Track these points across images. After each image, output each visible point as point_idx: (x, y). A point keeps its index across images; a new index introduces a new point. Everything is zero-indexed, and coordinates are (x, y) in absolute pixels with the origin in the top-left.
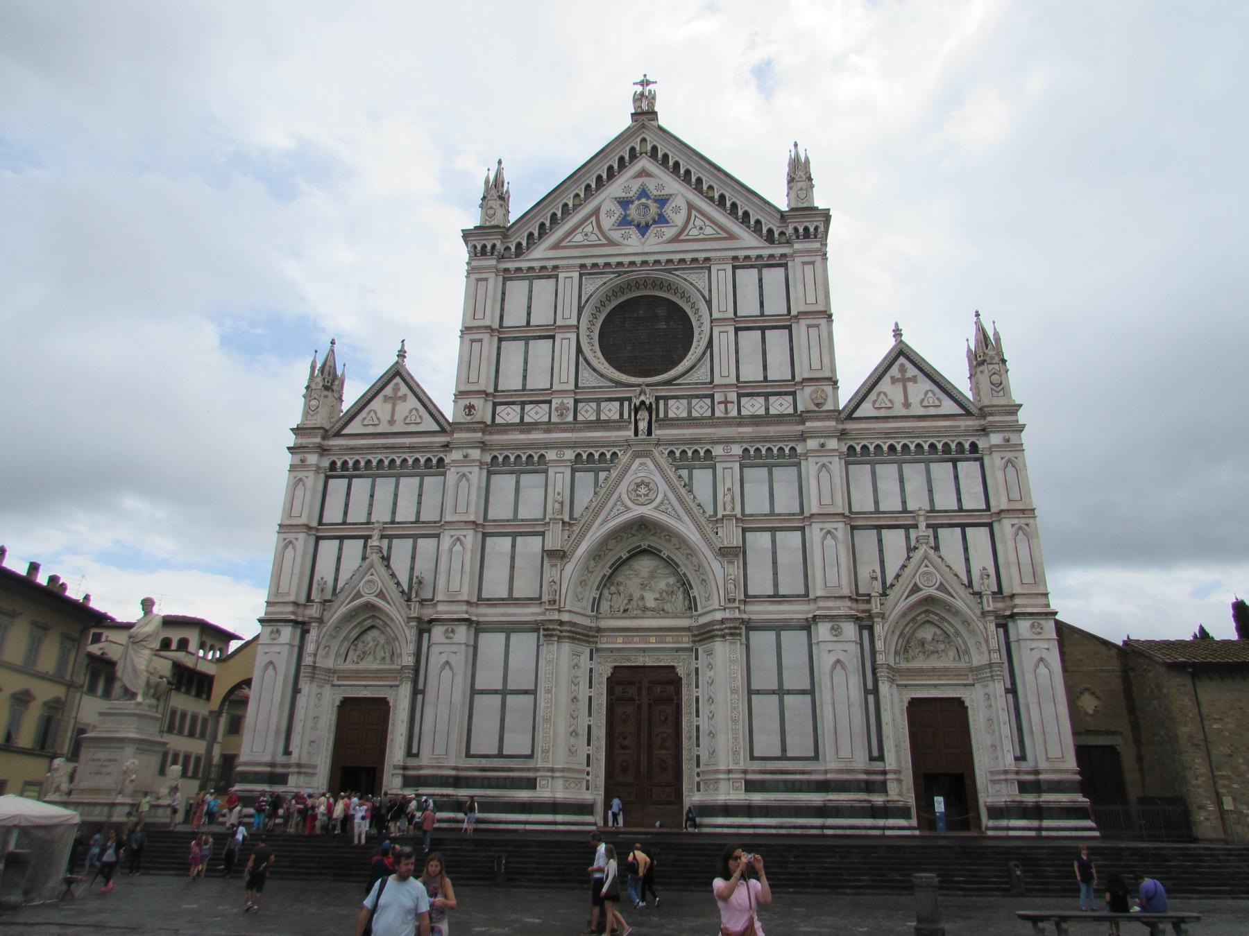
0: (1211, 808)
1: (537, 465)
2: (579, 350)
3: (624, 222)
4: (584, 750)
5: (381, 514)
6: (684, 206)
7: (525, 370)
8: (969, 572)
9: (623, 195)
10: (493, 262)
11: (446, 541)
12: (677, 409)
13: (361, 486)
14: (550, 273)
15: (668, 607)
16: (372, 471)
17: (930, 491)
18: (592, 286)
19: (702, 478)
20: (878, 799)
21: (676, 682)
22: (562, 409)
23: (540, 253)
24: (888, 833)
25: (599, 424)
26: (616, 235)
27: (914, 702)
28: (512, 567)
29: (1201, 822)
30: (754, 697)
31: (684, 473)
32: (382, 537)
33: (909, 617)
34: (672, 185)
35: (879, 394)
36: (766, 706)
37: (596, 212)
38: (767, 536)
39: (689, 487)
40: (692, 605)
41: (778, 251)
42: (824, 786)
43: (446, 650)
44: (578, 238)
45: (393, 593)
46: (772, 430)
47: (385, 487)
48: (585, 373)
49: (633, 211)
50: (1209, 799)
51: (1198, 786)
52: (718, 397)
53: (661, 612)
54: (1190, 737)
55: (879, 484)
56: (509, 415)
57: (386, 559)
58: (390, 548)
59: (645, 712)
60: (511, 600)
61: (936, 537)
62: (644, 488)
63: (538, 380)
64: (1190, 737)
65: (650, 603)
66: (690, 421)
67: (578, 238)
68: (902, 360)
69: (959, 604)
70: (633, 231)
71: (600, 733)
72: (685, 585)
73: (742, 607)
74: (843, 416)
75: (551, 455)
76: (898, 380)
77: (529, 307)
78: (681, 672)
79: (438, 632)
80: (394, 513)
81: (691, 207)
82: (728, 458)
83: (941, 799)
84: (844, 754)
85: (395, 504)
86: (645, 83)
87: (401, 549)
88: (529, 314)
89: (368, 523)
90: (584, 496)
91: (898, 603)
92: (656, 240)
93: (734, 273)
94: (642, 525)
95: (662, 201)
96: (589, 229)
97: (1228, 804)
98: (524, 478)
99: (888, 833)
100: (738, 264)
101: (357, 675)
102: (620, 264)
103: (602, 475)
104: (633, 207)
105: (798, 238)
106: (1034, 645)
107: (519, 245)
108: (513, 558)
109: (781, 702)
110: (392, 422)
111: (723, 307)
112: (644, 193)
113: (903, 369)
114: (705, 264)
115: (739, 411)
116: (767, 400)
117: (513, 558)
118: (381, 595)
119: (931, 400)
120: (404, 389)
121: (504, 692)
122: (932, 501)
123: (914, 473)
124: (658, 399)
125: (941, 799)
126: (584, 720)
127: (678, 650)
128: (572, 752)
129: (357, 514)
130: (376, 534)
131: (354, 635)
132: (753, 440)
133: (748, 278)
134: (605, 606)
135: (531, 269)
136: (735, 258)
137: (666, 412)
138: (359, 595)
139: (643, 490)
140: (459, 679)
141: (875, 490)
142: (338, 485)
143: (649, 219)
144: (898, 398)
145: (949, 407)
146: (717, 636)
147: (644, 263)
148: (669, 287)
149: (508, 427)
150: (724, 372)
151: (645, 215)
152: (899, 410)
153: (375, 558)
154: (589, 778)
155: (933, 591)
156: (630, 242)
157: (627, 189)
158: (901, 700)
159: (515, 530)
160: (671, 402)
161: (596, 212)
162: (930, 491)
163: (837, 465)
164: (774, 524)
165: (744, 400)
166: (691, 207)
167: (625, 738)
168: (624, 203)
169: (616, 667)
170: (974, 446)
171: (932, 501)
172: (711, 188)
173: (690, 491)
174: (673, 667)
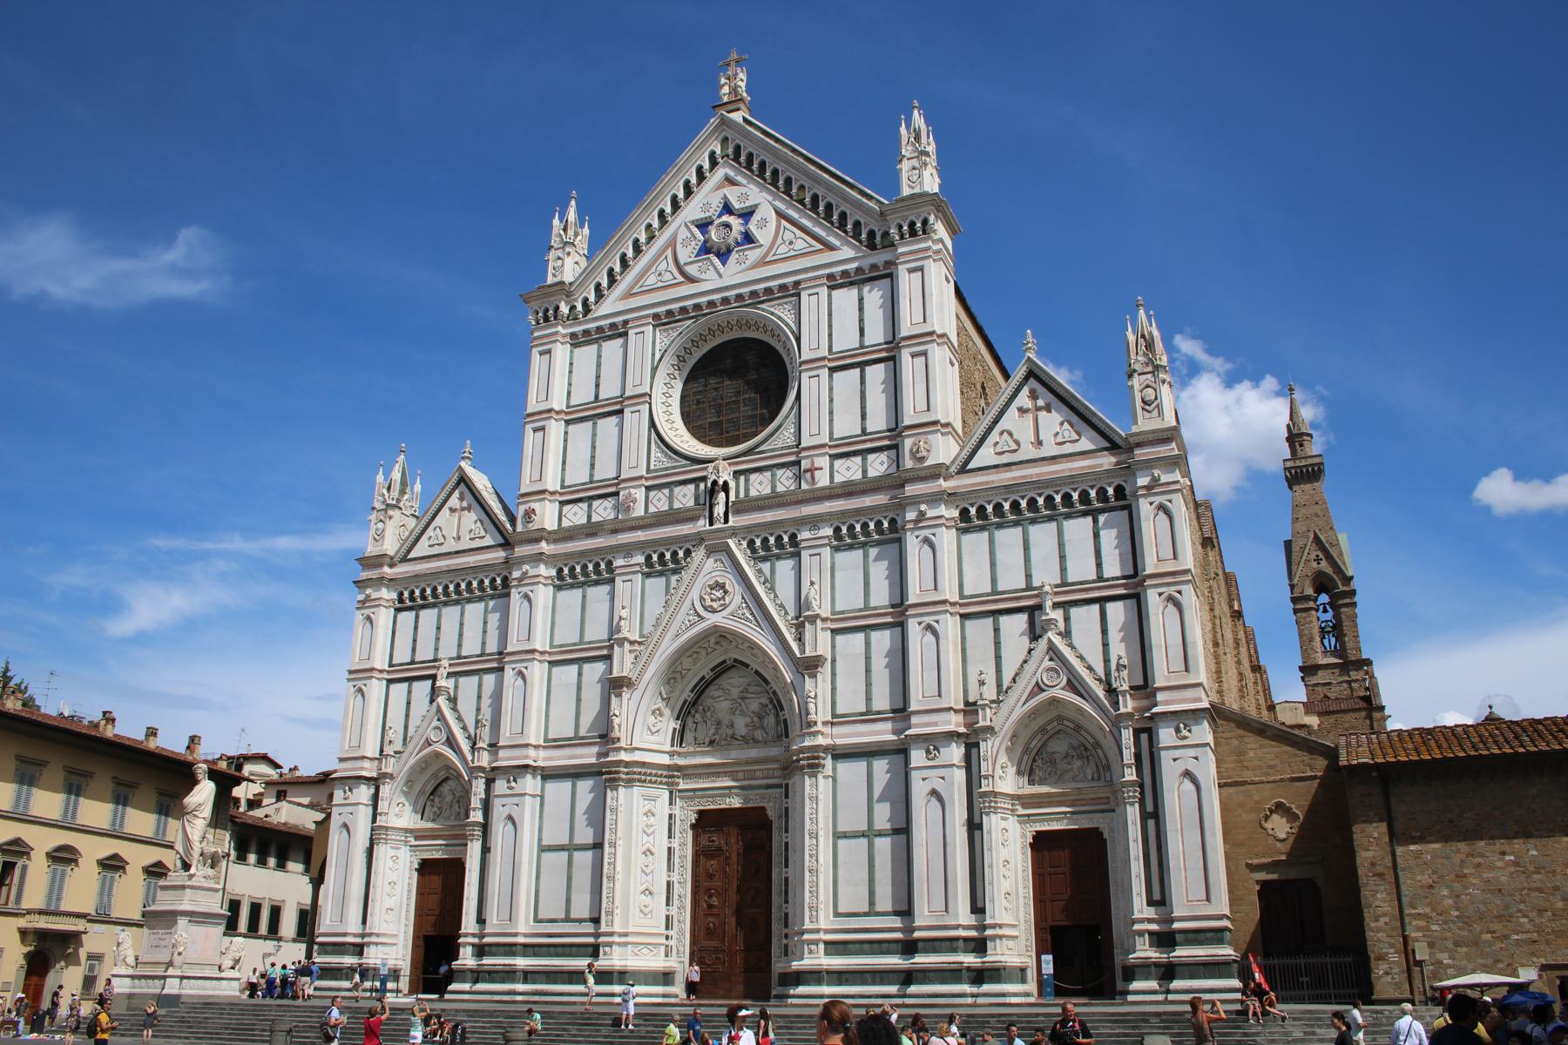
0: (1394, 957)
3: (706, 249)
4: (662, 911)
7: (593, 457)
8: (1107, 661)
9: (703, 215)
12: (759, 485)
14: (618, 331)
15: (759, 735)
17: (1062, 557)
19: (785, 567)
21: (766, 825)
24: (980, 1000)
26: (692, 270)
28: (579, 700)
29: (1379, 978)
30: (841, 842)
31: (766, 567)
32: (450, 675)
33: (1035, 726)
35: (1002, 433)
37: (672, 243)
41: (880, 258)
44: (651, 280)
49: (714, 235)
50: (1392, 946)
51: (1379, 930)
52: (805, 464)
53: (750, 741)
54: (1373, 864)
55: (999, 556)
57: (453, 701)
58: (456, 687)
61: (1067, 619)
64: (1373, 864)
67: (651, 280)
68: (1032, 380)
71: (684, 891)
72: (778, 705)
73: (827, 730)
74: (953, 469)
76: (1027, 411)
77: (598, 377)
78: (771, 813)
80: (460, 646)
83: (1050, 957)
85: (461, 635)
88: (597, 386)
89: (435, 660)
91: (1015, 708)
92: (739, 268)
93: (830, 296)
95: (747, 215)
96: (663, 266)
99: (980, 1000)
100: (836, 282)
102: (697, 307)
103: (674, 578)
105: (902, 237)
106: (1177, 753)
107: (585, 302)
108: (579, 689)
109: (871, 846)
112: (727, 209)
114: (791, 292)
115: (832, 477)
116: (864, 460)
117: (579, 689)
119: (1066, 434)
122: (1063, 570)
123: (1043, 535)
124: (737, 474)
125: (1050, 957)
127: (768, 787)
129: (425, 653)
131: (429, 789)
132: (844, 514)
133: (846, 298)
135: (600, 329)
136: (831, 277)
137: (747, 490)
138: (428, 743)
139: (719, 594)
141: (993, 565)
143: (731, 241)
146: (802, 768)
147: (725, 301)
148: (757, 324)
152: (1028, 452)
153: (442, 701)
154: (670, 942)
158: (1023, 836)
160: (753, 477)
161: (672, 243)
162: (1062, 557)
165: (837, 463)
167: (710, 897)
169: (701, 813)
171: (1063, 570)
172: (802, 187)
173: (772, 589)
174: (763, 809)
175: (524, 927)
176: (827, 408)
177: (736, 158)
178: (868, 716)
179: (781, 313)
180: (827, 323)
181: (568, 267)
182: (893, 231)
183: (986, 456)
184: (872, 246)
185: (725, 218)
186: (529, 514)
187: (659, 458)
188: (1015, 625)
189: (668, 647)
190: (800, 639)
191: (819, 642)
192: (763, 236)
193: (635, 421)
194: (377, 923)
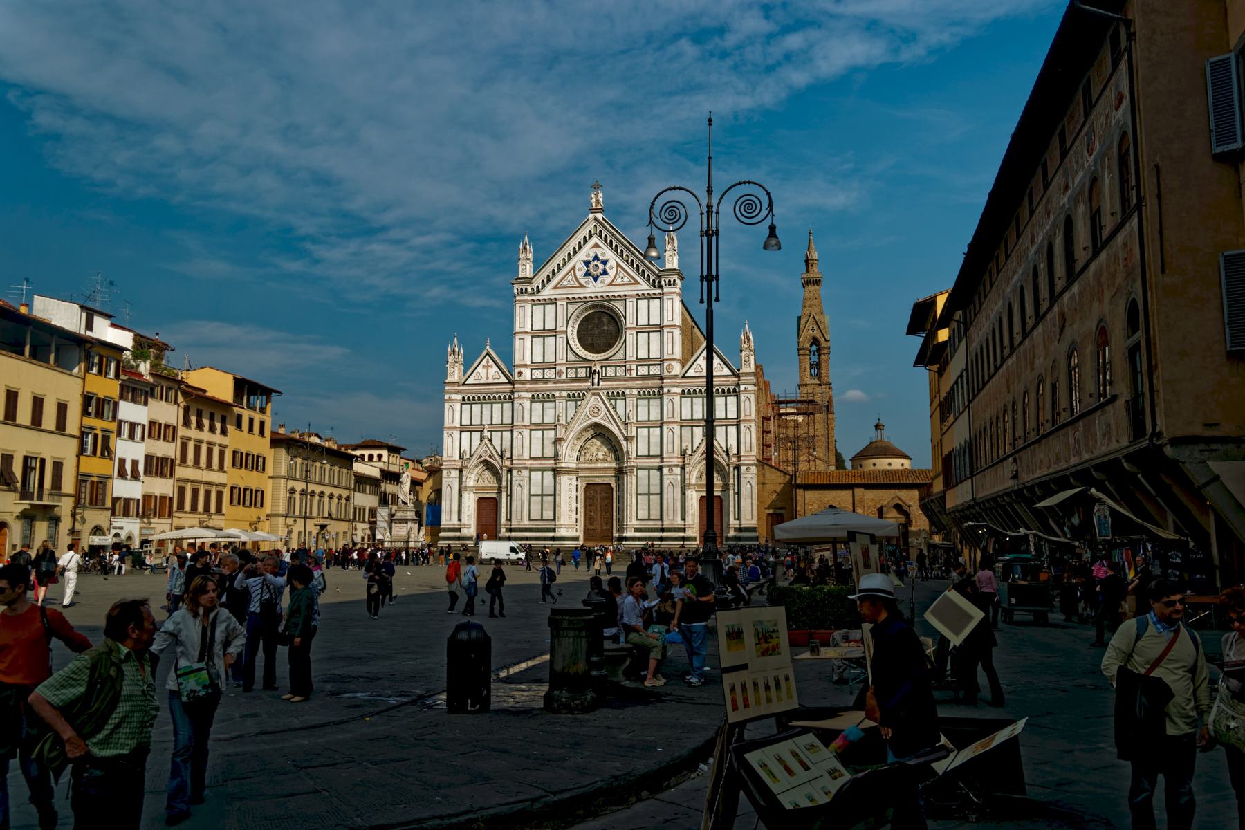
1: (554, 399)
2: (568, 343)
3: (587, 274)
4: (574, 517)
5: (486, 421)
6: (615, 265)
12: (610, 372)
13: (476, 407)
14: (553, 302)
16: (481, 401)
18: (571, 308)
19: (620, 403)
23: (548, 292)
25: (577, 380)
26: (583, 282)
36: (643, 500)
37: (573, 268)
39: (614, 408)
42: (662, 530)
43: (519, 479)
44: (565, 283)
46: (650, 383)
47: (486, 407)
53: (604, 460)
56: (538, 374)
59: (601, 501)
60: (543, 458)
62: (594, 409)
63: (550, 358)
65: (601, 456)
66: (616, 378)
67: (565, 283)
90: (571, 413)
94: (596, 425)
95: (605, 262)
98: (546, 405)
100: (639, 297)
101: (483, 488)
104: (591, 266)
111: (630, 322)
112: (596, 258)
114: (623, 299)
120: (491, 362)
121: (542, 495)
126: (574, 505)
128: (570, 517)
129: (476, 421)
142: (466, 407)
148: (608, 308)
149: (537, 381)
150: (631, 356)
156: (590, 285)
157: (587, 255)
159: (542, 427)
163: (677, 399)
164: (647, 424)
168: (587, 263)
175: (526, 523)
176: (635, 346)
178: (649, 456)
179: (619, 306)
180: (635, 313)
181: (526, 270)
183: (691, 373)
186: (520, 373)
187: (571, 357)
189: (577, 428)
190: (627, 430)
191: (632, 431)
192: (612, 273)
193: (561, 340)
194: (465, 520)
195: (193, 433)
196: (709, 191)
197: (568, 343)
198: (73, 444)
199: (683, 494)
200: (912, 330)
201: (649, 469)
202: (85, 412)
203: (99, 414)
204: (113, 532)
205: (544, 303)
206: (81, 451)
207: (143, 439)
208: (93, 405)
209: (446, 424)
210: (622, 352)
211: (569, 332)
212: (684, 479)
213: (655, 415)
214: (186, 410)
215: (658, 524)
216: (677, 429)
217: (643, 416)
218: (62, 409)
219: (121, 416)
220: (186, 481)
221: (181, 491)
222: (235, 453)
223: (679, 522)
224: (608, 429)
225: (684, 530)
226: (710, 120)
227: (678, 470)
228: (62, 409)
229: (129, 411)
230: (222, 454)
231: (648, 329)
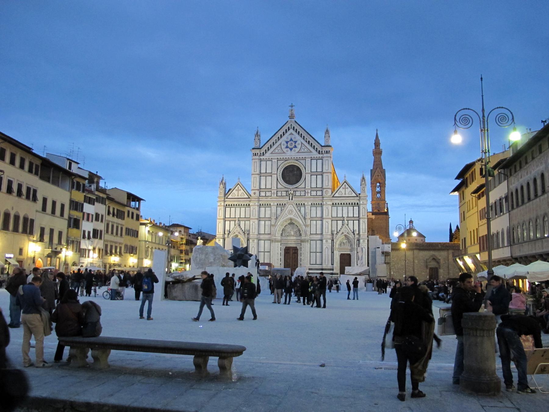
2: (277, 179)
3: (287, 147)
4: (280, 262)
5: (238, 216)
10: (257, 157)
11: (251, 223)
14: (271, 160)
18: (280, 162)
19: (302, 209)
20: (331, 271)
22: (274, 193)
23: (268, 155)
26: (285, 150)
27: (341, 254)
34: (298, 138)
36: (313, 255)
37: (281, 144)
38: (315, 222)
39: (300, 211)
40: (301, 235)
41: (321, 156)
42: (322, 269)
45: (241, 232)
47: (238, 210)
48: (279, 184)
57: (239, 225)
59: (291, 255)
62: (290, 212)
63: (269, 186)
67: (277, 151)
69: (351, 236)
70: (289, 149)
72: (299, 231)
75: (272, 204)
79: (251, 241)
81: (302, 143)
82: (308, 205)
84: (327, 264)
86: (292, 106)
87: (242, 223)
90: (279, 212)
94: (291, 219)
97: (392, 273)
104: (289, 143)
110: (238, 196)
111: (308, 171)
112: (291, 140)
113: (345, 186)
118: (239, 233)
121: (264, 252)
123: (345, 209)
128: (277, 263)
129: (233, 216)
130: (237, 220)
134: (283, 234)
140: (256, 250)
143: (292, 146)
144: (344, 192)
145: (354, 195)
151: (291, 145)
153: (237, 225)
155: (346, 234)
157: (287, 138)
159: (265, 219)
161: (281, 144)
163: (330, 207)
166: (302, 143)
168: (287, 142)
170: (358, 204)
177: (294, 129)
182: (323, 152)
183: (337, 195)
184: (319, 153)
185: (291, 142)
188: (340, 223)
189: (282, 220)
192: (299, 147)
195: (110, 218)
196: (483, 110)
197: (277, 179)
198: (66, 222)
199: (332, 252)
200: (458, 178)
201: (316, 241)
202: (70, 208)
203: (76, 209)
204: (81, 264)
205: (266, 161)
206: (69, 226)
207: (92, 221)
208: (76, 206)
209: (218, 217)
210: (304, 184)
211: (278, 174)
212: (333, 246)
213: (319, 215)
214: (109, 207)
215: (320, 267)
216: (330, 221)
217: (314, 215)
218: (63, 206)
219: (84, 211)
220: (107, 241)
221: (106, 246)
222: (126, 228)
223: (330, 266)
224: (296, 221)
225: (333, 270)
226: (482, 79)
227: (330, 241)
228: (63, 206)
229: (88, 208)
230: (122, 228)
231: (316, 174)
